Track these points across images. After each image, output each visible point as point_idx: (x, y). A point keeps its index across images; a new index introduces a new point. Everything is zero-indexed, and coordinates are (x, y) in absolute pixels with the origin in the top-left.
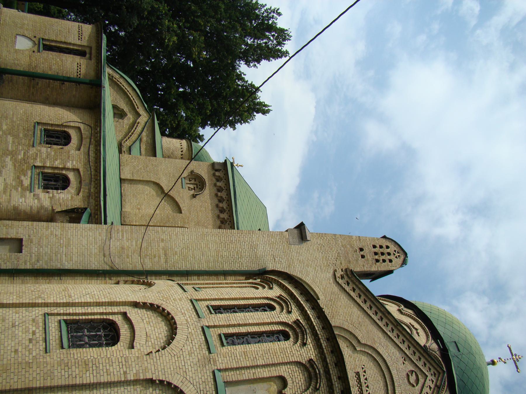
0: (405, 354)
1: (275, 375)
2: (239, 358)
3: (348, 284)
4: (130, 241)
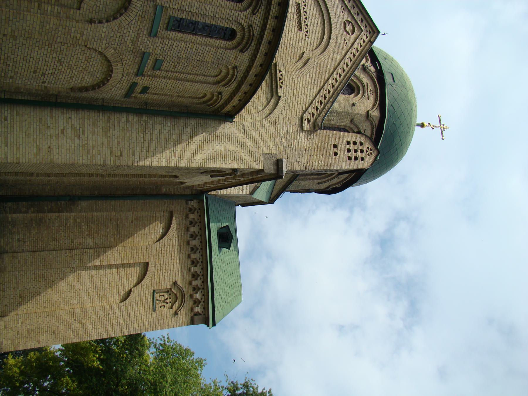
0: (345, 5)
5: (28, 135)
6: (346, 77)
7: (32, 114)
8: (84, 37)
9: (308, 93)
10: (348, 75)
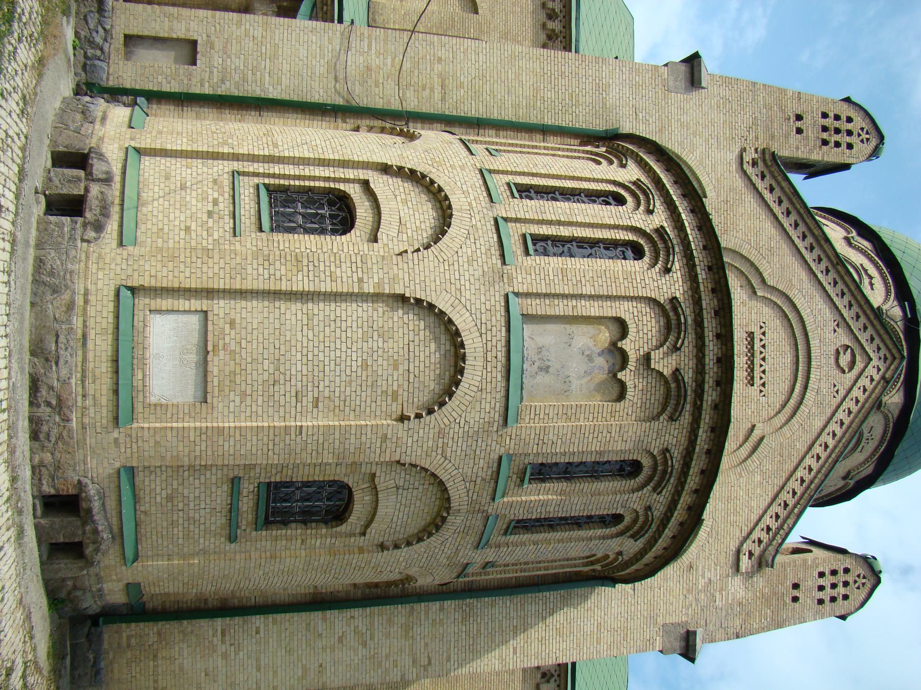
0: (842, 315)
1: (610, 315)
2: (552, 278)
3: (763, 177)
4: (381, 57)
5: (289, 652)
6: (830, 461)
7: (295, 619)
8: (372, 565)
9: (754, 504)
10: (833, 456)
